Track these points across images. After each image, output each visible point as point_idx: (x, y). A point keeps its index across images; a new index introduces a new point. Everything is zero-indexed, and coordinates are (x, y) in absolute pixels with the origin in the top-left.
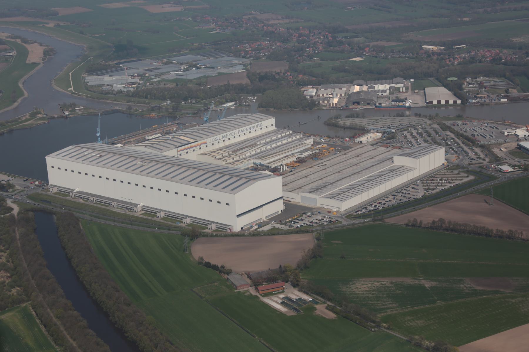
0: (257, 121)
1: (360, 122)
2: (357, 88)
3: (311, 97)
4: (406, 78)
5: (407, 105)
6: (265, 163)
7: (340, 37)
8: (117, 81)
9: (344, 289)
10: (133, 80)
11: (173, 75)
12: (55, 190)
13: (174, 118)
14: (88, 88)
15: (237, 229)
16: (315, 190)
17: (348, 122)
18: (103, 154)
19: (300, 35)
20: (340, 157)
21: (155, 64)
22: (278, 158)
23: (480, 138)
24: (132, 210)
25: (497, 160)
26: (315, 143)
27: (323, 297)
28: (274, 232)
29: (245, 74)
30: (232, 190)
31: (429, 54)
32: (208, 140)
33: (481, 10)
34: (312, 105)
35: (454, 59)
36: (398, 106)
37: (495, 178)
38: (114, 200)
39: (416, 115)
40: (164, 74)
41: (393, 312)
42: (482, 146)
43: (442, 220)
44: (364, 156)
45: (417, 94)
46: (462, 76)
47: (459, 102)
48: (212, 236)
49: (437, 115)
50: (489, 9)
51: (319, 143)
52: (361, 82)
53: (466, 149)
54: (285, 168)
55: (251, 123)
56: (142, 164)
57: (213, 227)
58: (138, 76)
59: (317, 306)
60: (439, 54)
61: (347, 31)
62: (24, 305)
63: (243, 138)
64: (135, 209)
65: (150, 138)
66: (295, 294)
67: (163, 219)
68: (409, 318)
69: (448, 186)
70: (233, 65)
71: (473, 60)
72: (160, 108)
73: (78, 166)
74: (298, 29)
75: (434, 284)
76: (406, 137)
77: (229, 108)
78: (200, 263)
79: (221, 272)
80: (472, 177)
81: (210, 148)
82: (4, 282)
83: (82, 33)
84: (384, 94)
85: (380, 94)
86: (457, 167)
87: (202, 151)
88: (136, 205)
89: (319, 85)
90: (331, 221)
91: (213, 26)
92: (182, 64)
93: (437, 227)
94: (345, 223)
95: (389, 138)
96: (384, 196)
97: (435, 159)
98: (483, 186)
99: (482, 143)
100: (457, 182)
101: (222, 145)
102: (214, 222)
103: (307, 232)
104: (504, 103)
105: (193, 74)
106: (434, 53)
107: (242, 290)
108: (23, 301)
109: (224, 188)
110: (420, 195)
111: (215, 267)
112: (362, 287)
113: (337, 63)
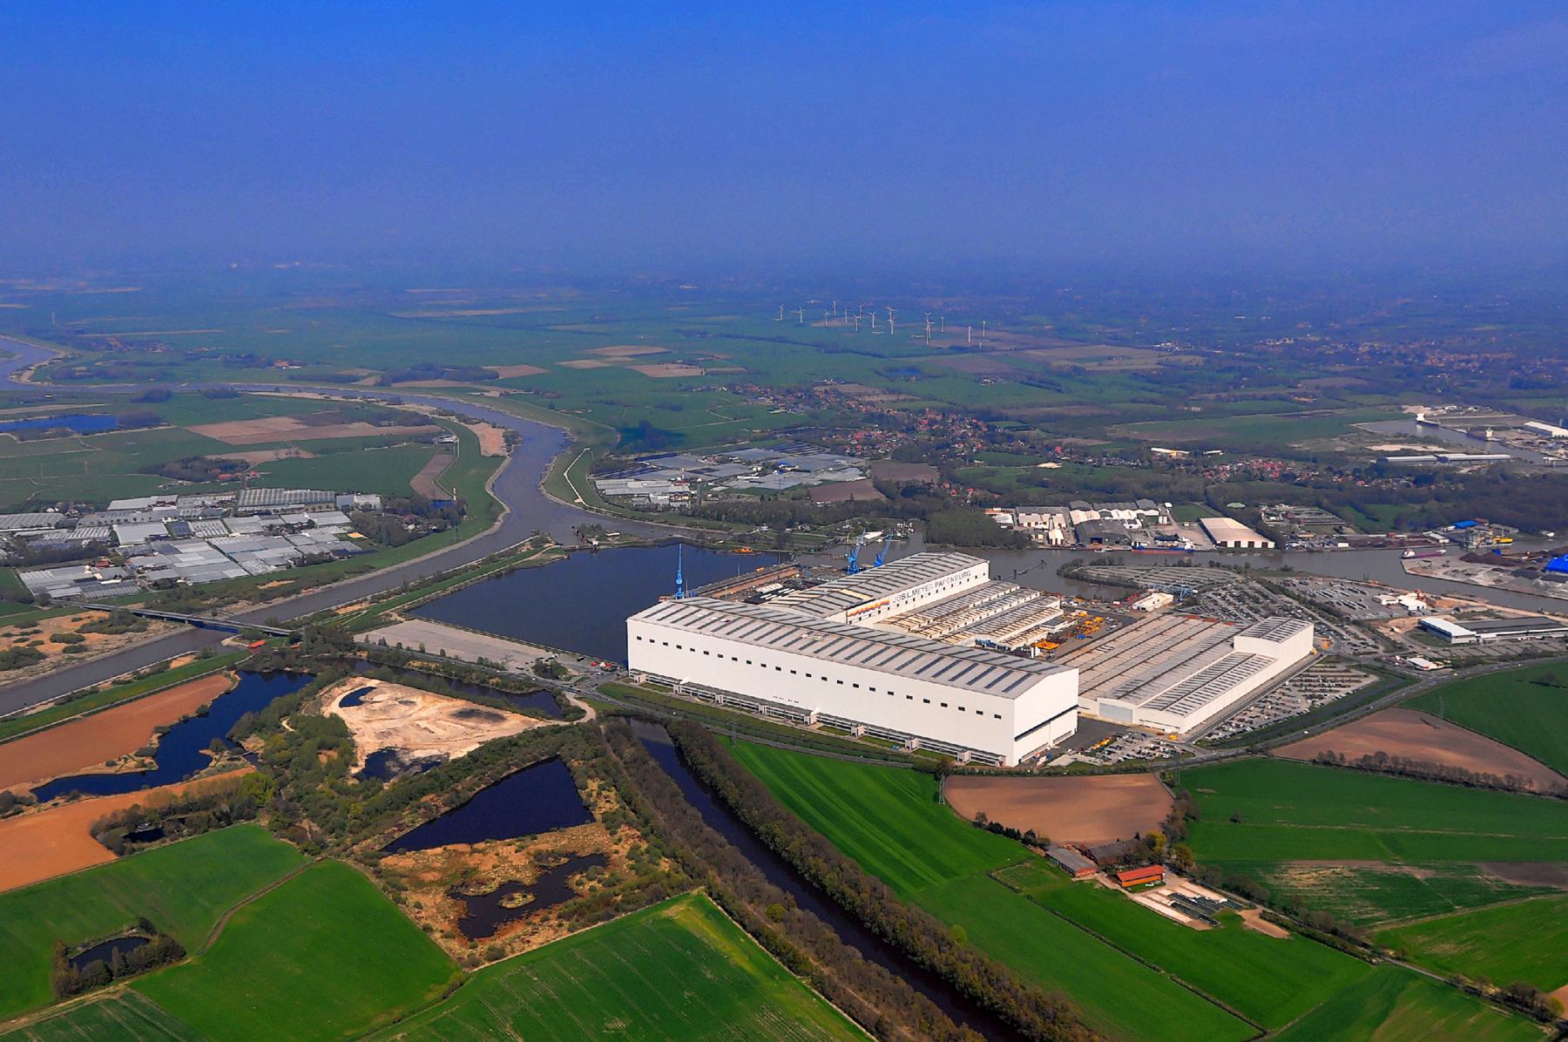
0: (961, 568)
1: (1127, 573)
2: (1080, 517)
3: (1010, 527)
4: (1159, 500)
5: (1188, 547)
6: (998, 640)
7: (1001, 427)
8: (657, 488)
9: (1271, 881)
10: (680, 489)
11: (742, 482)
12: (643, 679)
13: (786, 557)
14: (607, 499)
15: (1012, 762)
16: (1125, 694)
17: (1105, 573)
18: (731, 618)
19: (932, 422)
20: (1126, 637)
21: (705, 462)
22: (1017, 632)
23: (1344, 609)
24: (800, 720)
25: (1395, 647)
26: (1068, 609)
27: (1248, 897)
28: (1077, 770)
29: (870, 484)
30: (1006, 690)
31: (1173, 464)
32: (891, 598)
33: (1212, 396)
34: (1018, 542)
35: (1217, 472)
36: (1172, 548)
37: (1416, 680)
39: (1212, 565)
40: (727, 479)
41: (1388, 928)
42: (1355, 623)
43: (1381, 756)
44: (1173, 633)
45: (1190, 528)
46: (1252, 501)
47: (1271, 545)
48: (972, 773)
49: (1247, 566)
50: (1223, 395)
51: (1073, 610)
52: (1086, 504)
53: (1333, 627)
54: (1038, 652)
55: (953, 570)
57: (967, 756)
58: (685, 481)
59: (1242, 913)
60: (1188, 464)
61: (1007, 419)
62: (695, 892)
63: (942, 595)
64: (806, 719)
65: (765, 590)
66: (1191, 891)
67: (862, 737)
68: (1421, 939)
69: (1343, 693)
70: (842, 469)
71: (1248, 476)
72: (754, 538)
73: (689, 637)
74: (923, 412)
75: (1430, 873)
76: (1216, 603)
77: (874, 541)
78: (978, 825)
79: (1025, 841)
80: (1373, 678)
81: (895, 612)
82: (635, 848)
83: (551, 407)
84: (1135, 527)
85: (1127, 526)
86: (1338, 658)
87: (881, 617)
88: (808, 713)
89: (1013, 507)
90: (1173, 752)
91: (769, 401)
92: (749, 463)
93: (1366, 767)
94: (1199, 756)
95: (1189, 604)
96: (1242, 706)
97: (1299, 644)
98: (1403, 693)
99: (1354, 617)
100: (1356, 686)
101: (911, 606)
102: (967, 749)
103: (1144, 770)
104: (1343, 550)
105: (773, 481)
106: (1177, 462)
107: (1088, 877)
108: (692, 886)
109: (989, 686)
110: (1304, 706)
111: (1012, 834)
112: (1302, 877)
113: (1021, 471)
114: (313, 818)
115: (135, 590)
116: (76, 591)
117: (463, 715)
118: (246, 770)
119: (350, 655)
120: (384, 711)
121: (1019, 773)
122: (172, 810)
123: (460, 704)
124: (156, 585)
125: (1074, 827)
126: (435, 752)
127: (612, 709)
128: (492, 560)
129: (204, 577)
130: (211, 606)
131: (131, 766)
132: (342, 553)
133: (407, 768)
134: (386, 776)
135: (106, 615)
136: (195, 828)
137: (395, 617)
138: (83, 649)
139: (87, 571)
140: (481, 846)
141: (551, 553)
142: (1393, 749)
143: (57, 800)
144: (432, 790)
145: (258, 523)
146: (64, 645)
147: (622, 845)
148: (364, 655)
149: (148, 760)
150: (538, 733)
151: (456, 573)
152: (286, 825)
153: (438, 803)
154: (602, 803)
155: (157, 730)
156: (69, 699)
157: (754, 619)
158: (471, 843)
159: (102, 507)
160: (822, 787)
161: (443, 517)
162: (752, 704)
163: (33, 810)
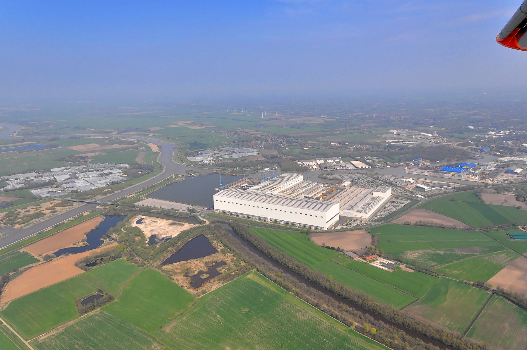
15: (325, 229)
16: (351, 208)
28: (343, 230)
38: (254, 216)
43: (420, 221)
48: (316, 232)
56: (266, 198)
81: (282, 190)
87: (279, 191)
93: (416, 225)
103: (360, 229)
114: (139, 256)
115: (66, 194)
116: (49, 195)
117: (172, 224)
118: (115, 244)
119: (134, 209)
120: (149, 224)
121: (329, 232)
122: (97, 257)
123: (170, 221)
124: (72, 192)
125: (350, 245)
126: (168, 235)
127: (213, 220)
128: (166, 180)
129: (86, 189)
130: (90, 197)
131: (81, 244)
132: (123, 180)
133: (161, 240)
134: (157, 243)
135: (60, 201)
136: (106, 261)
137: (143, 198)
138: (56, 211)
139: (50, 189)
140: (189, 261)
141: (181, 178)
142: (422, 220)
143: (62, 256)
144: (170, 246)
145: (95, 173)
146: (50, 211)
147: (229, 258)
148: (138, 209)
149: (85, 243)
150: (195, 228)
151: (157, 185)
152: (131, 258)
153: (173, 250)
154: (219, 247)
155: (85, 234)
156: (57, 226)
157: (248, 194)
158: (186, 260)
159: (49, 171)
160: (277, 238)
161: (149, 170)
162: (251, 217)
163: (55, 259)
